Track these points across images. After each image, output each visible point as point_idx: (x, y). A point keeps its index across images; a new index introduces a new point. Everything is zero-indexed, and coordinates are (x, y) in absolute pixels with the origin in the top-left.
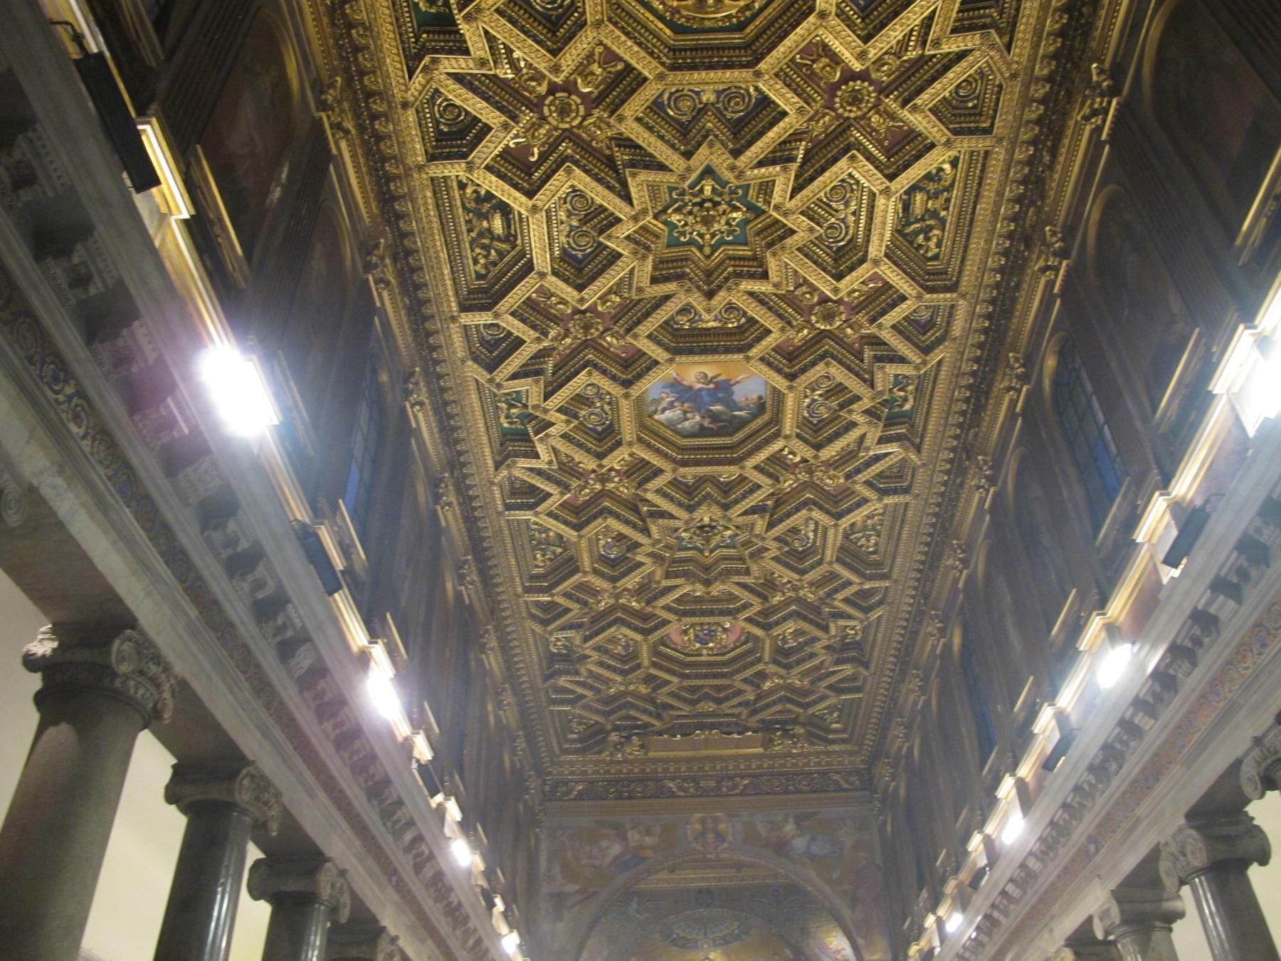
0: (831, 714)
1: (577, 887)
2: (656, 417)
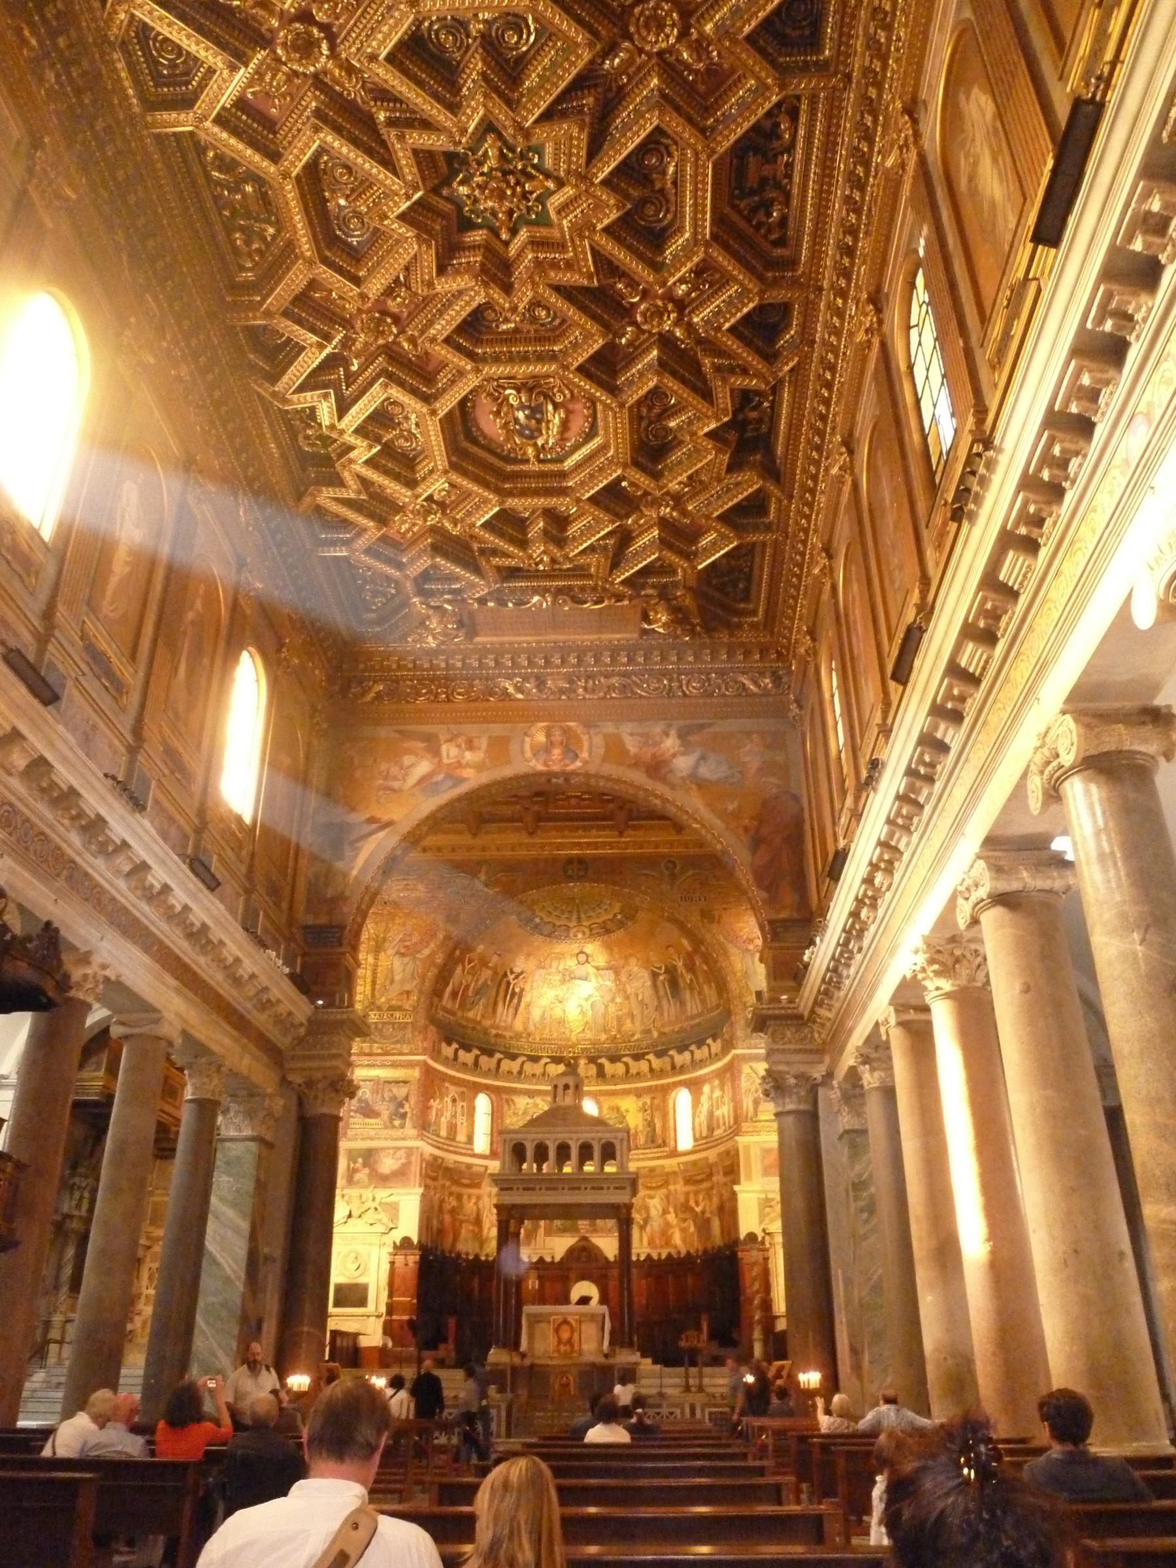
0: (735, 584)
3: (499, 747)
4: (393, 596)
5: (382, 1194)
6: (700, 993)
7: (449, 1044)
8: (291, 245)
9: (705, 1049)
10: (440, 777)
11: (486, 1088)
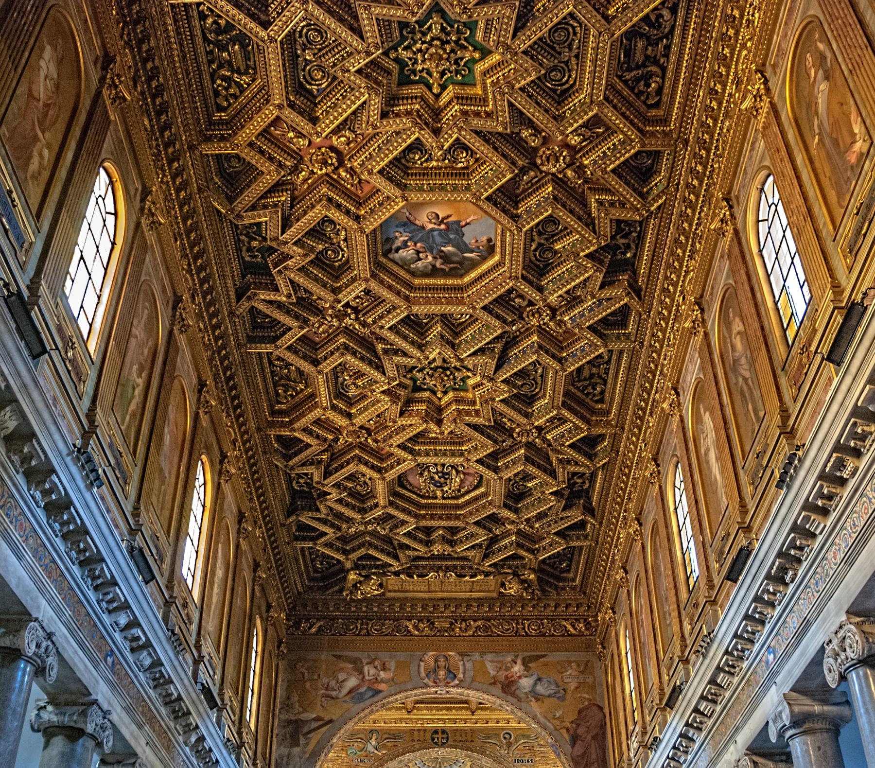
1: (314, 716)
2: (391, 256)
4: (334, 565)
8: (312, 396)
10: (363, 690)
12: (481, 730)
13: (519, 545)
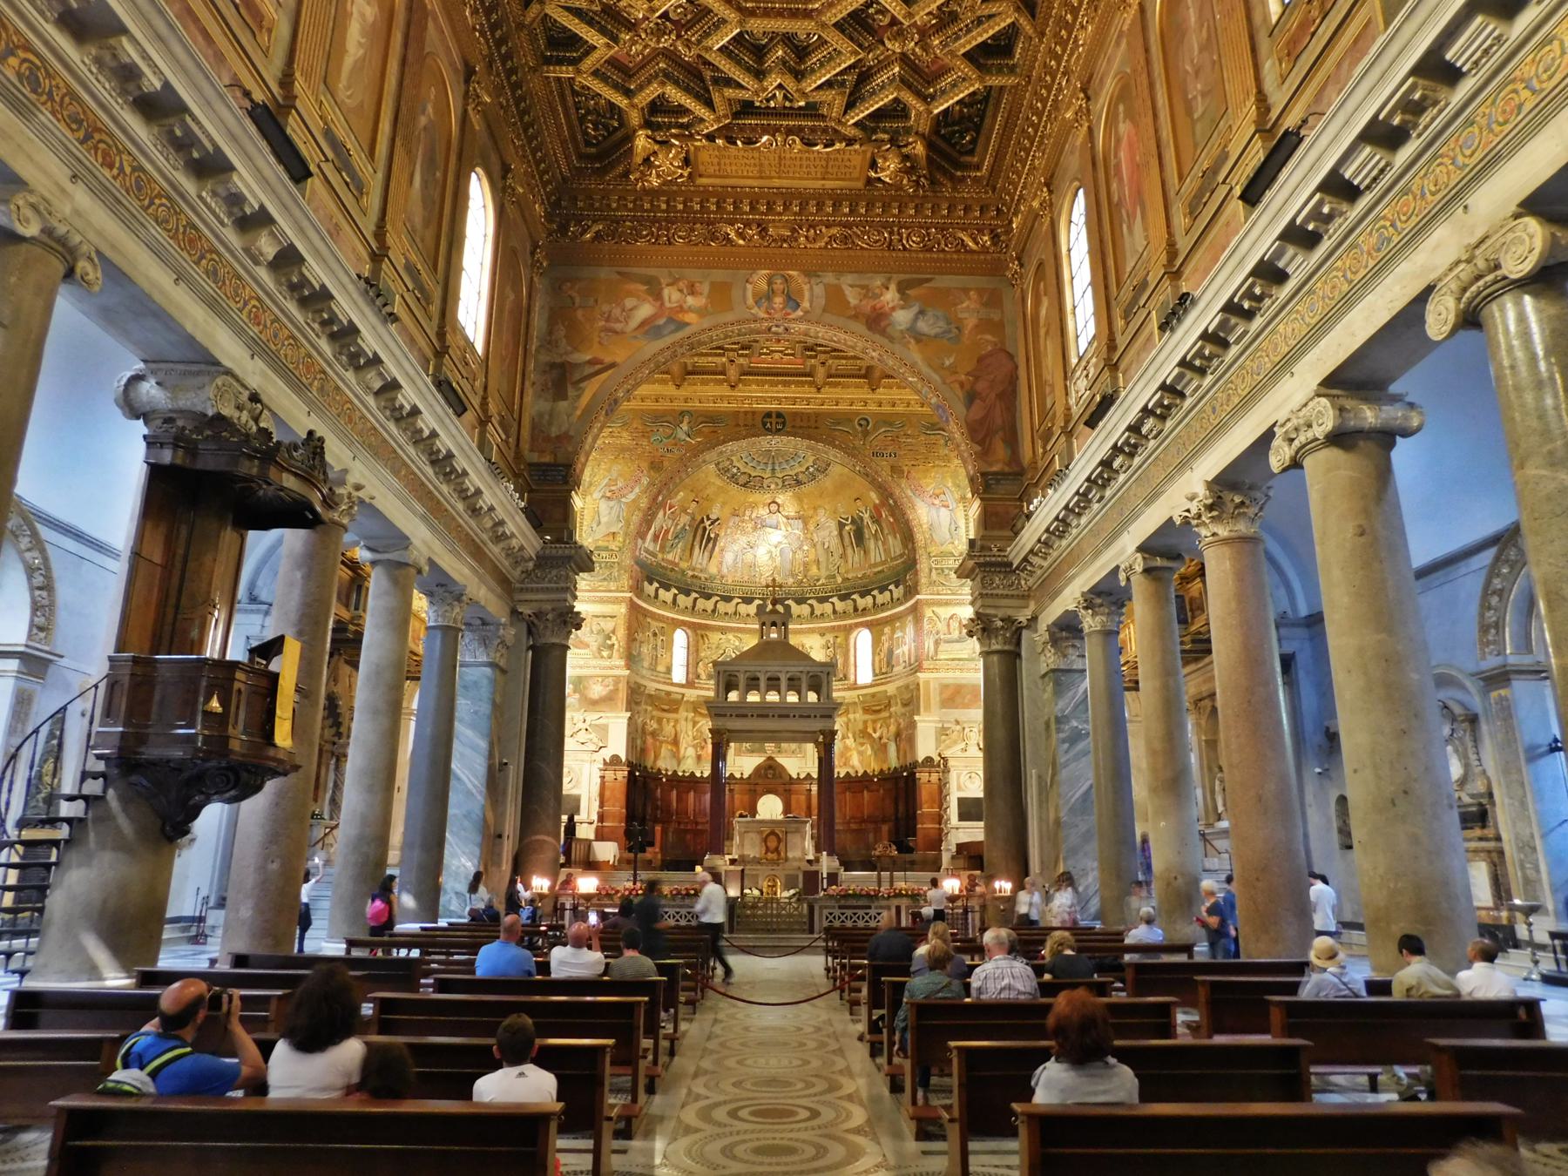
1: (588, 357)
3: (721, 295)
4: (616, 129)
5: (592, 717)
6: (884, 544)
7: (651, 584)
9: (887, 594)
10: (661, 321)
11: (682, 624)
12: (830, 414)
13: (904, 82)
